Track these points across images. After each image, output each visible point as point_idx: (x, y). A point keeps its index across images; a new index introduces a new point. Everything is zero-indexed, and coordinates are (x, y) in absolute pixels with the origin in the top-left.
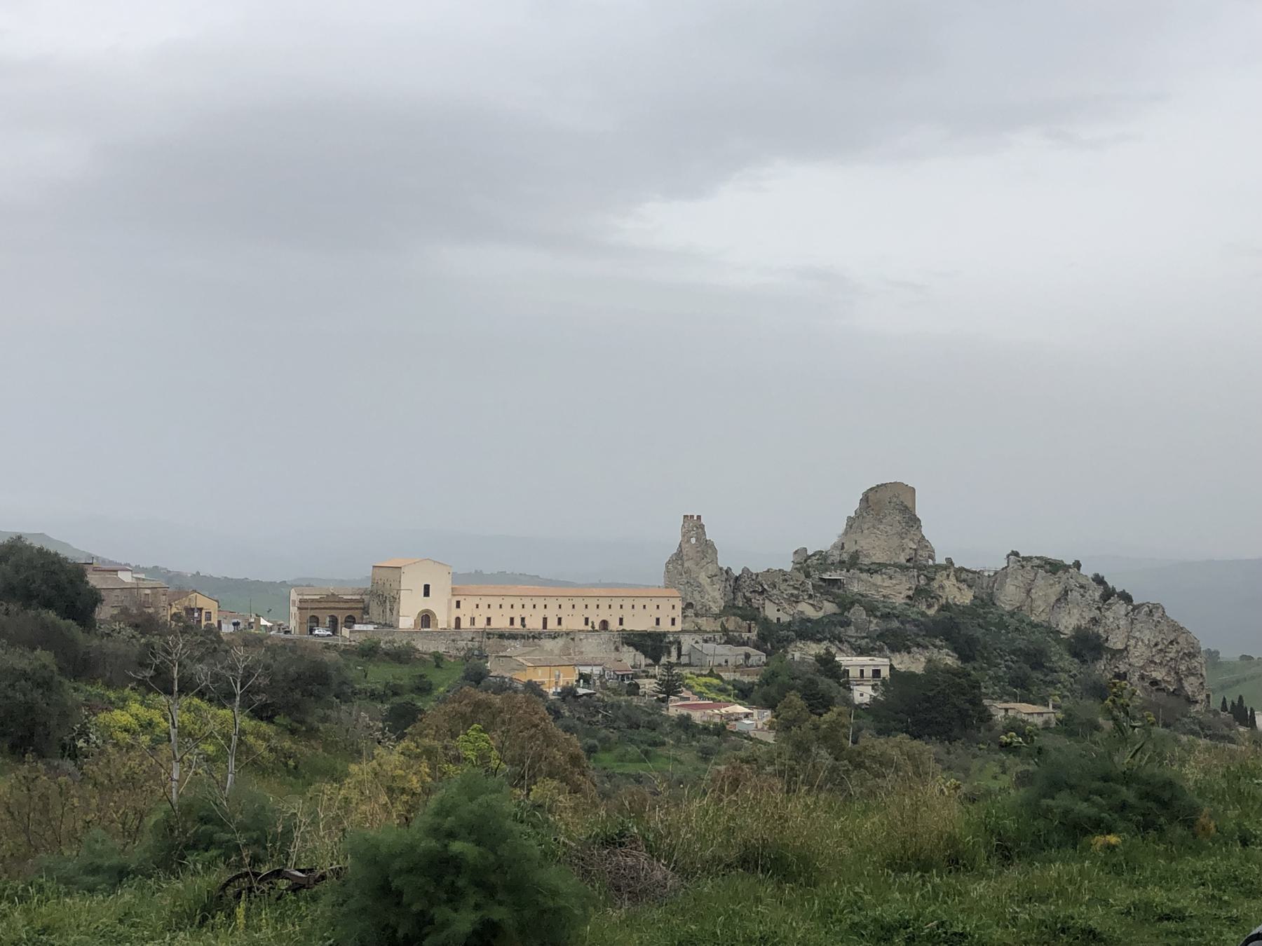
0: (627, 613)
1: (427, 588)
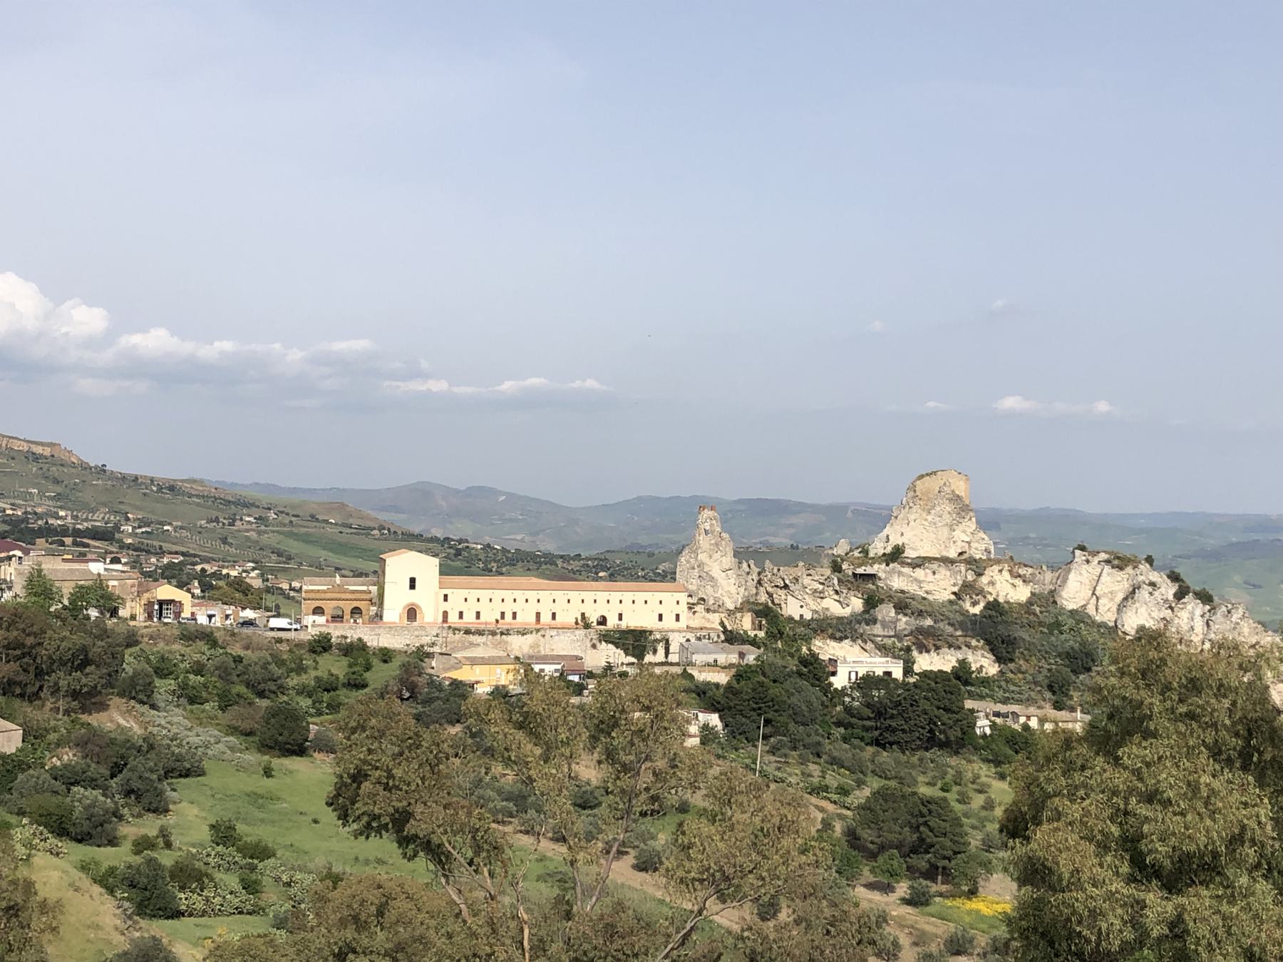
0: (626, 609)
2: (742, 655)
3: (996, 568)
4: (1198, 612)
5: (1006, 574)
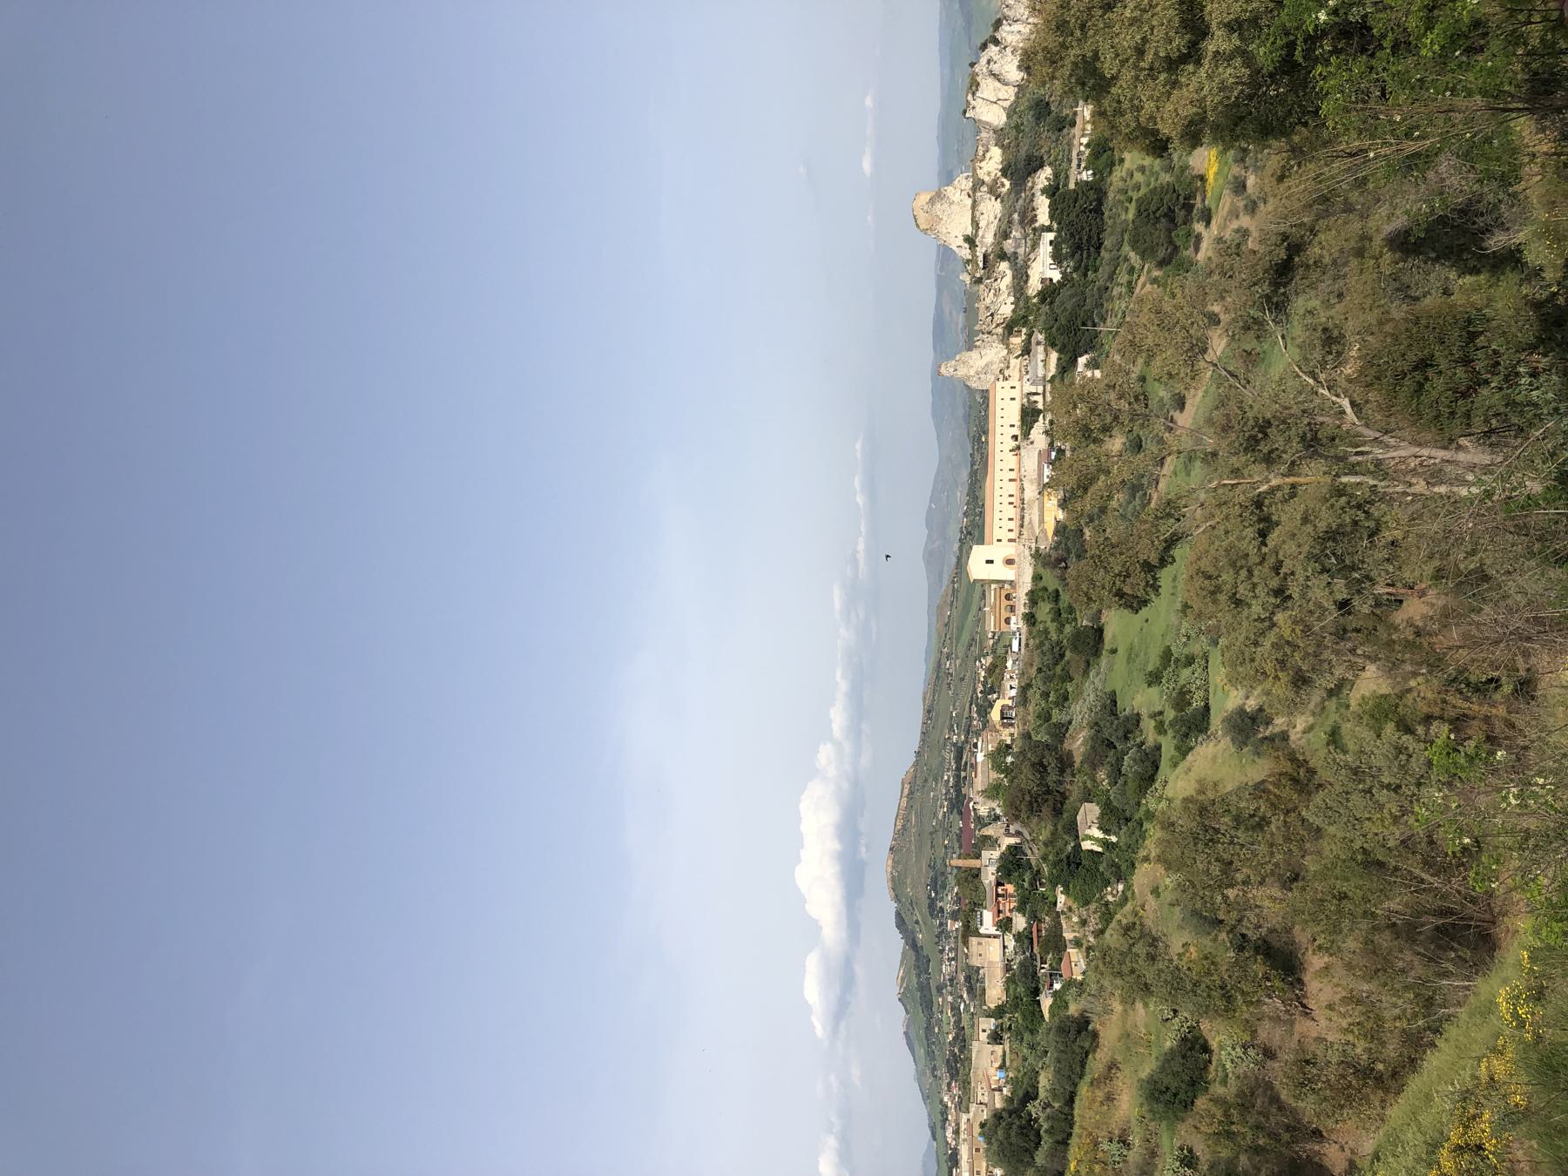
0: (1007, 422)
1: (992, 562)
2: (1038, 343)
3: (979, 171)
4: (1007, 28)
5: (983, 164)
